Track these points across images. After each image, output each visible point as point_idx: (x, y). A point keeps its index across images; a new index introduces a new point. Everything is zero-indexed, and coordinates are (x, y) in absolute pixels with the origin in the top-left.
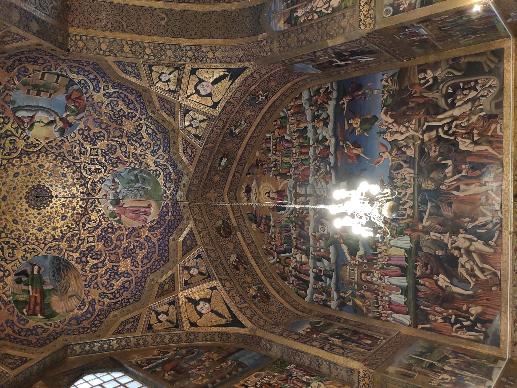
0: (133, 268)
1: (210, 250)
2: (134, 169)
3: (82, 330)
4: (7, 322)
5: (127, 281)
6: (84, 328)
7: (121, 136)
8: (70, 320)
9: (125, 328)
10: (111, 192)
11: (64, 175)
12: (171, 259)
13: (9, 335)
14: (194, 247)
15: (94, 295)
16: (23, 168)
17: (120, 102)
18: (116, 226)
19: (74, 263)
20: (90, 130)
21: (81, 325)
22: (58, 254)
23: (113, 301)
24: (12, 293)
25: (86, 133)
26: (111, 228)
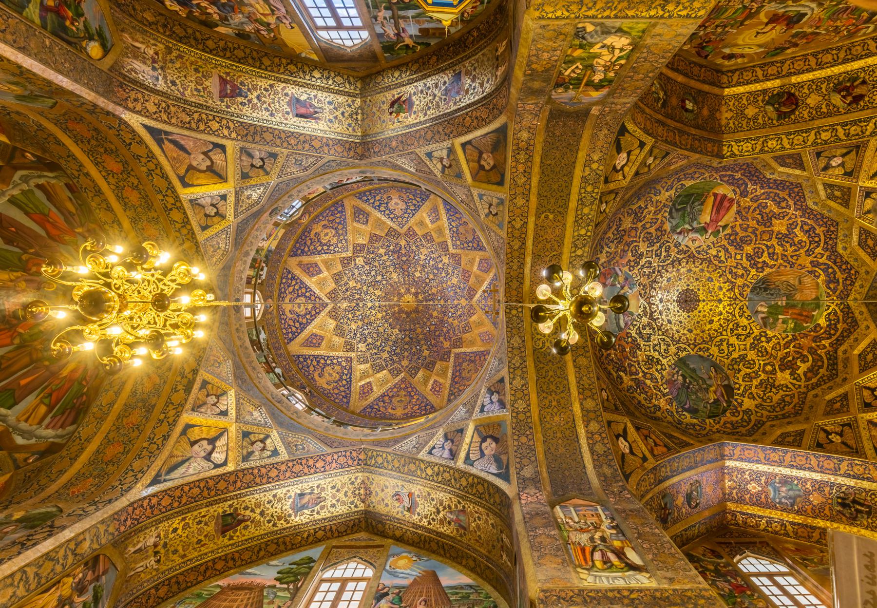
0: (787, 218)
1: (816, 138)
2: (670, 213)
3: (848, 282)
4: (815, 341)
5: (802, 227)
6: (846, 279)
7: (636, 229)
8: (829, 288)
9: (871, 245)
10: (692, 235)
11: (669, 280)
12: (799, 181)
13: (831, 344)
14: (801, 157)
15: (805, 261)
16: (664, 317)
17: (607, 236)
18: (728, 231)
19: (761, 275)
20: (630, 260)
21: (841, 281)
22: (748, 287)
23: (822, 245)
24: (784, 332)
25: (632, 264)
26: (730, 235)
